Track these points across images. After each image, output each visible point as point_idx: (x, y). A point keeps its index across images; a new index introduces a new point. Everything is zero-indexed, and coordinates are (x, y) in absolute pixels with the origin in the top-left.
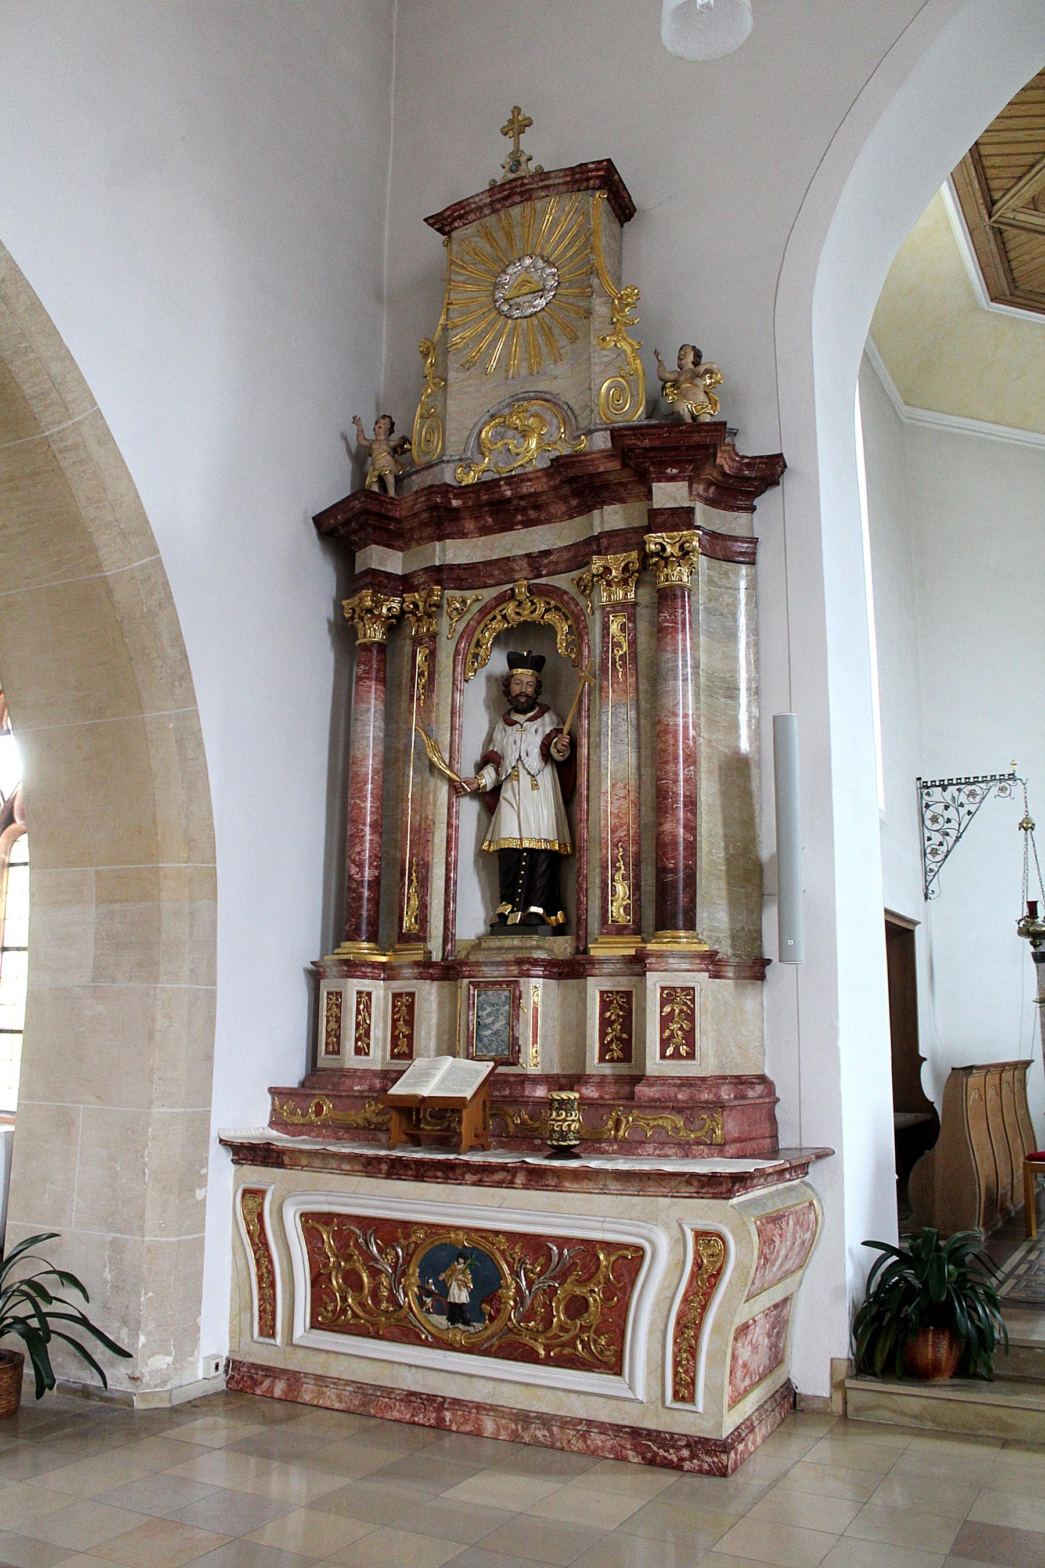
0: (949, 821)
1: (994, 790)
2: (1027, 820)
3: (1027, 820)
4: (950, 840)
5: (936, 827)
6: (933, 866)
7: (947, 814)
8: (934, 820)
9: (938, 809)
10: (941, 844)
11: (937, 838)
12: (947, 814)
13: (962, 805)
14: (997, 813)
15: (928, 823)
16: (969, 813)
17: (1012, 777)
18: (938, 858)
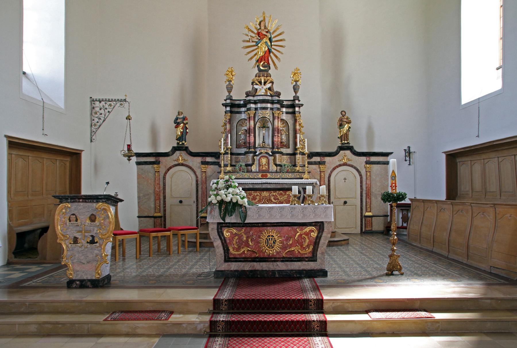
0: (101, 114)
1: (118, 104)
2: (129, 116)
3: (129, 116)
4: (101, 121)
5: (96, 116)
6: (94, 130)
7: (101, 112)
8: (96, 113)
9: (97, 109)
10: (98, 122)
11: (96, 120)
12: (101, 112)
13: (106, 109)
14: (119, 113)
15: (93, 114)
16: (109, 112)
17: (125, 100)
18: (96, 127)
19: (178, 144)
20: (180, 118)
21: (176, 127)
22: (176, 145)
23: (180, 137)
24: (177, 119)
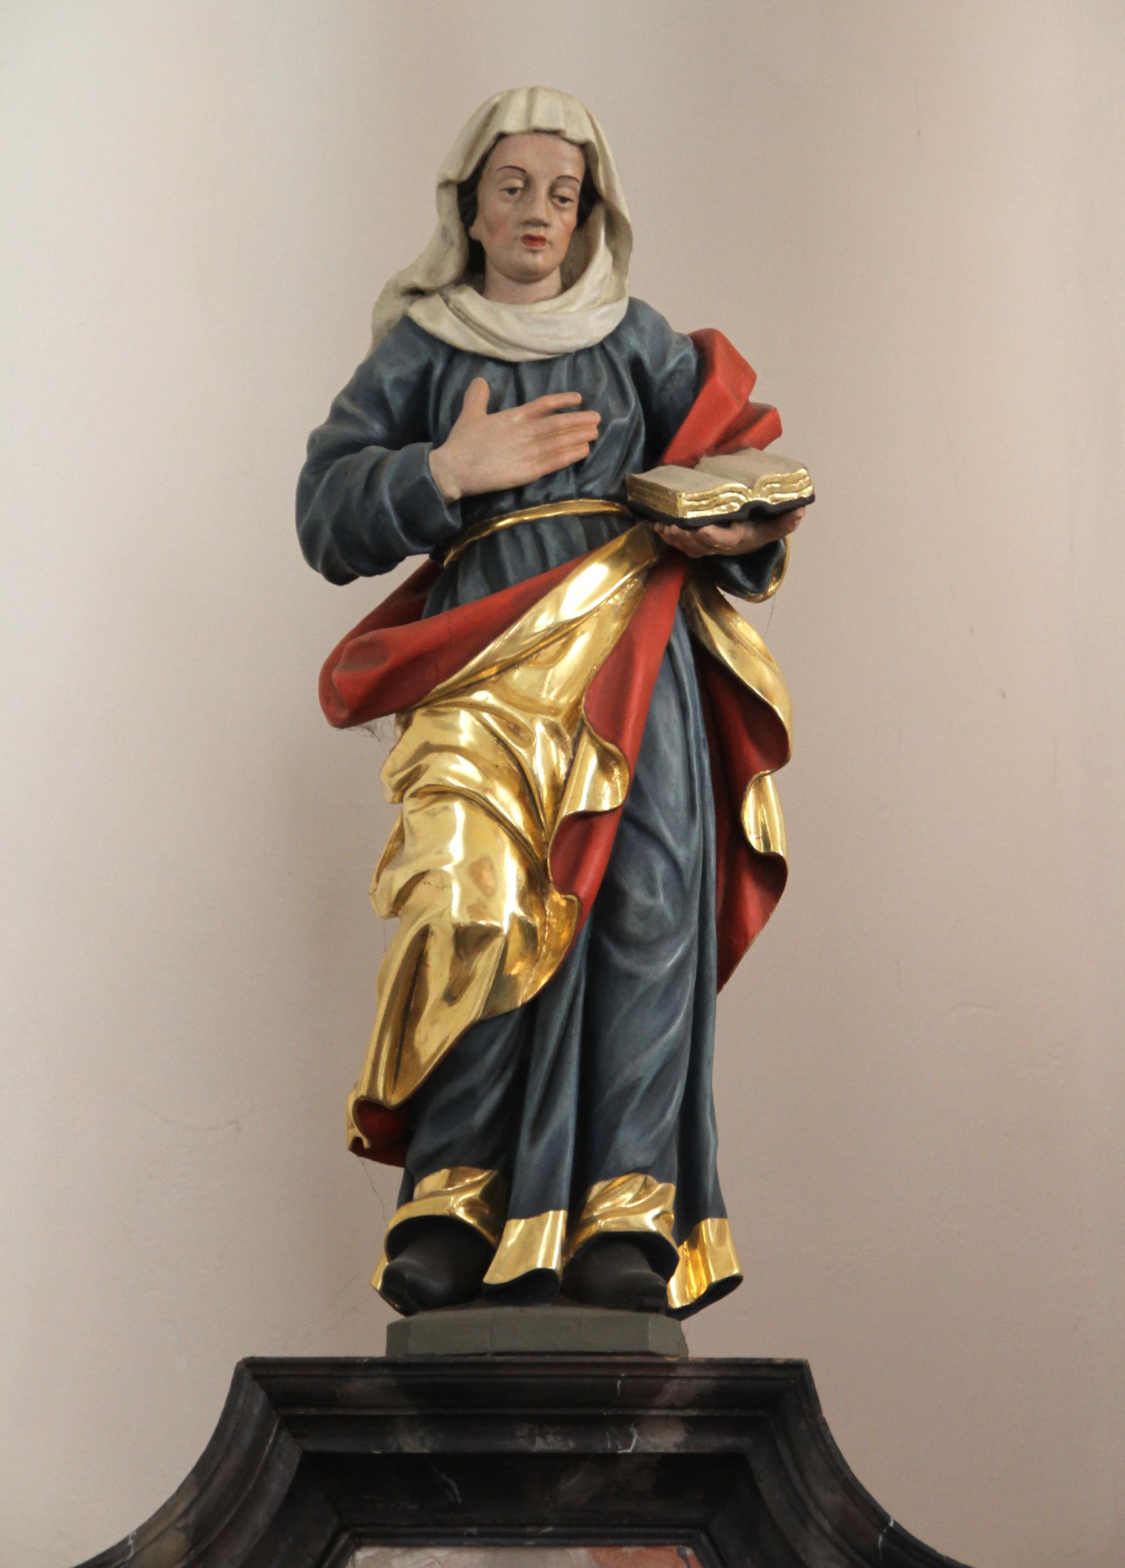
19: (436, 1263)
20: (518, 381)
21: (379, 685)
22: (358, 1327)
23: (513, 1036)
24: (409, 393)
